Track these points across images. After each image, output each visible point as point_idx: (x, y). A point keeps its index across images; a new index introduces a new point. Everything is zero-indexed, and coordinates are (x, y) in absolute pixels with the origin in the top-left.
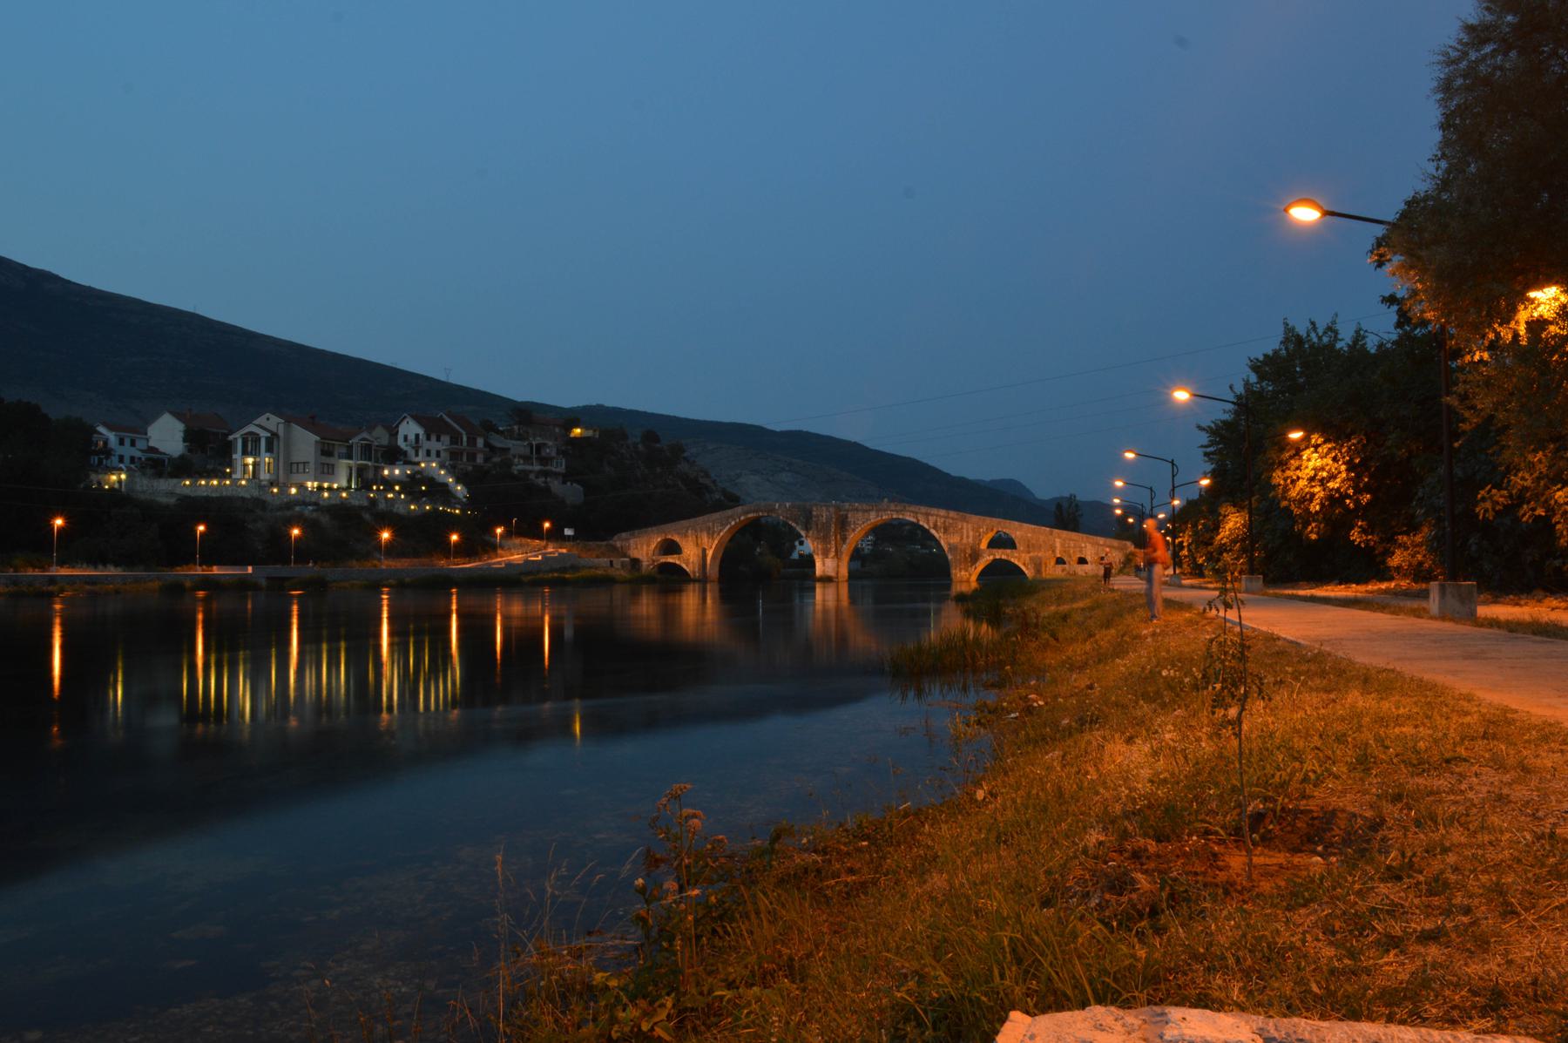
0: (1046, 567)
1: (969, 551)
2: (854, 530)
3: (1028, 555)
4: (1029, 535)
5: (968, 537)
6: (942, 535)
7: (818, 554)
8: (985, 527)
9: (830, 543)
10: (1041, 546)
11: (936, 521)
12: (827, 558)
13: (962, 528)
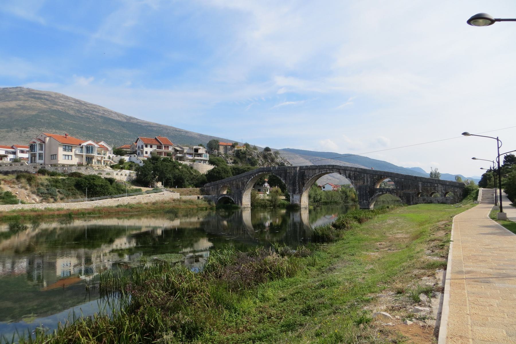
0: (413, 198)
1: (368, 190)
2: (308, 179)
4: (403, 180)
5: (367, 182)
6: (353, 181)
7: (290, 192)
8: (377, 176)
9: (296, 187)
10: (409, 185)
11: (350, 174)
13: (364, 177)
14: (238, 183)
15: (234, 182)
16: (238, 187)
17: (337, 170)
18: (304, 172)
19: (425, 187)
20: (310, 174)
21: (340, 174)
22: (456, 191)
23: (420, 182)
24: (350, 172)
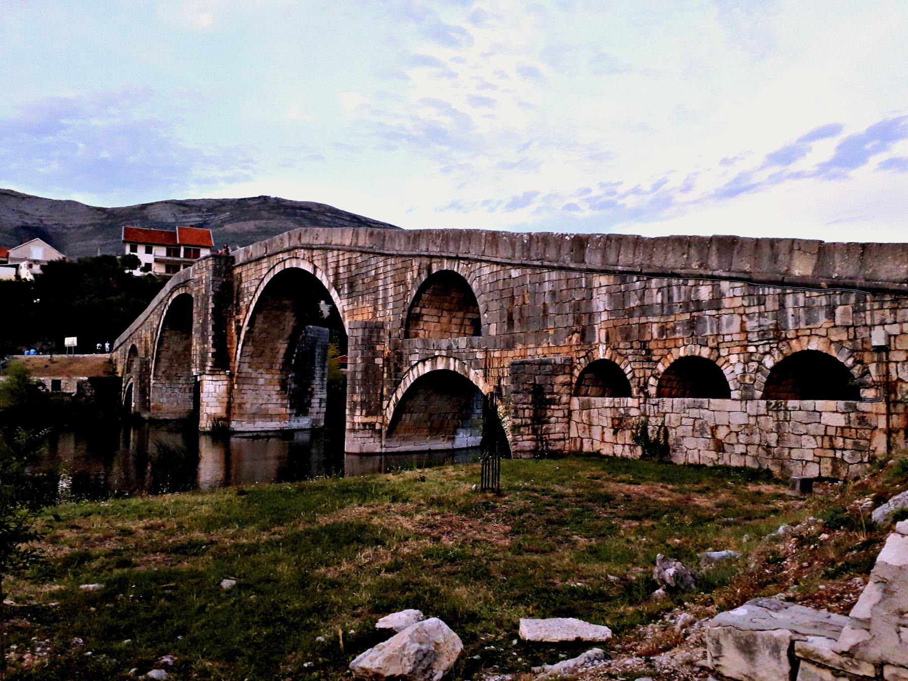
1: (385, 348)
3: (511, 354)
12: (204, 373)
13: (376, 278)
17: (307, 253)
18: (241, 274)
19: (630, 313)
22: (878, 338)
23: (603, 280)
24: (338, 255)
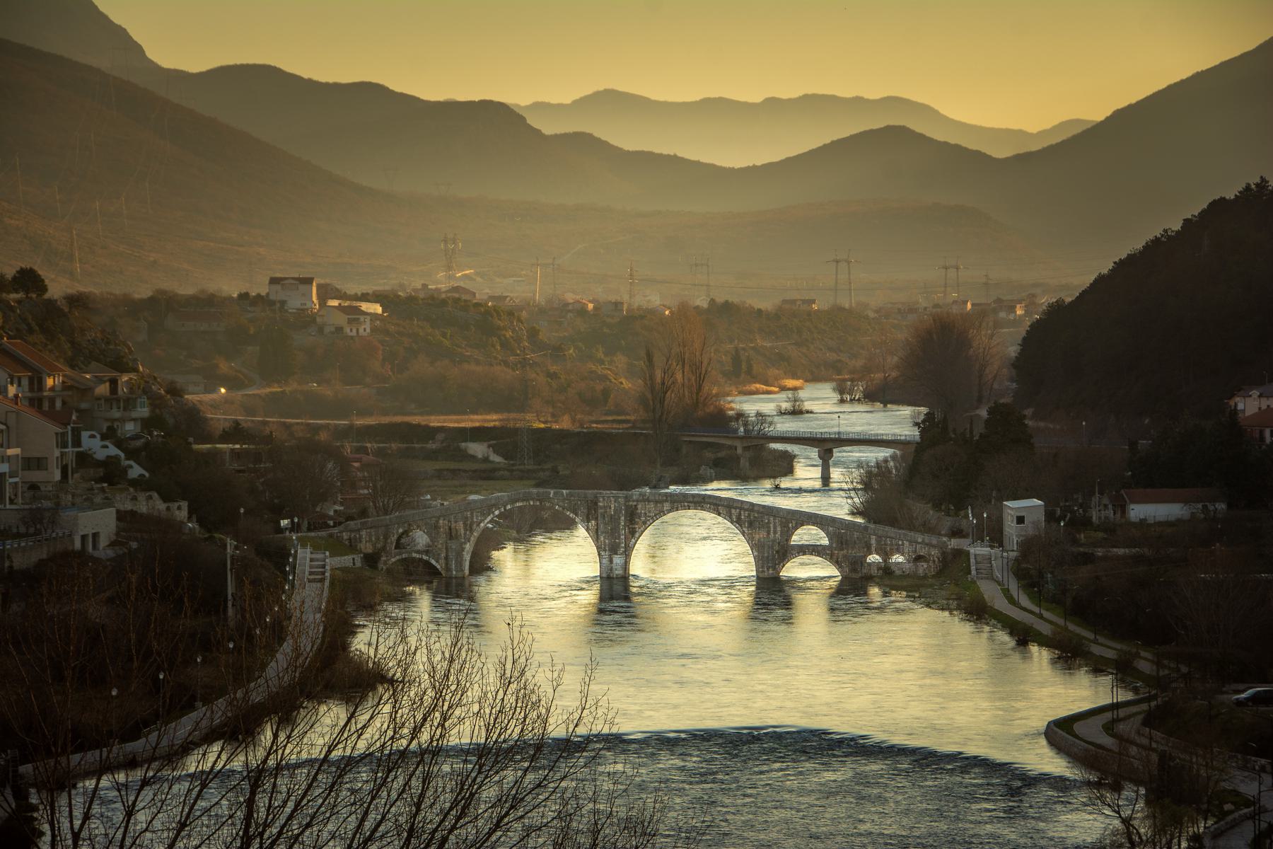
5: (775, 532)
7: (605, 550)
9: (619, 538)
11: (740, 514)
12: (616, 554)
13: (769, 523)
14: (453, 526)
15: (441, 522)
16: (454, 533)
20: (650, 512)
21: (719, 514)
